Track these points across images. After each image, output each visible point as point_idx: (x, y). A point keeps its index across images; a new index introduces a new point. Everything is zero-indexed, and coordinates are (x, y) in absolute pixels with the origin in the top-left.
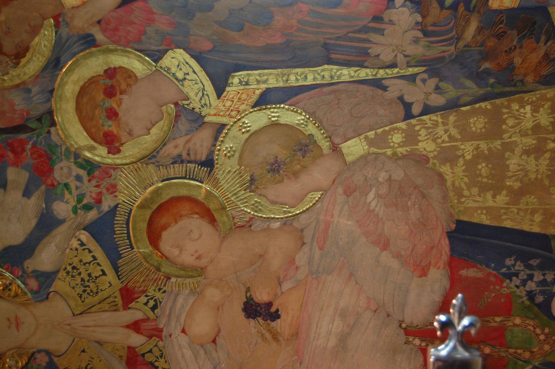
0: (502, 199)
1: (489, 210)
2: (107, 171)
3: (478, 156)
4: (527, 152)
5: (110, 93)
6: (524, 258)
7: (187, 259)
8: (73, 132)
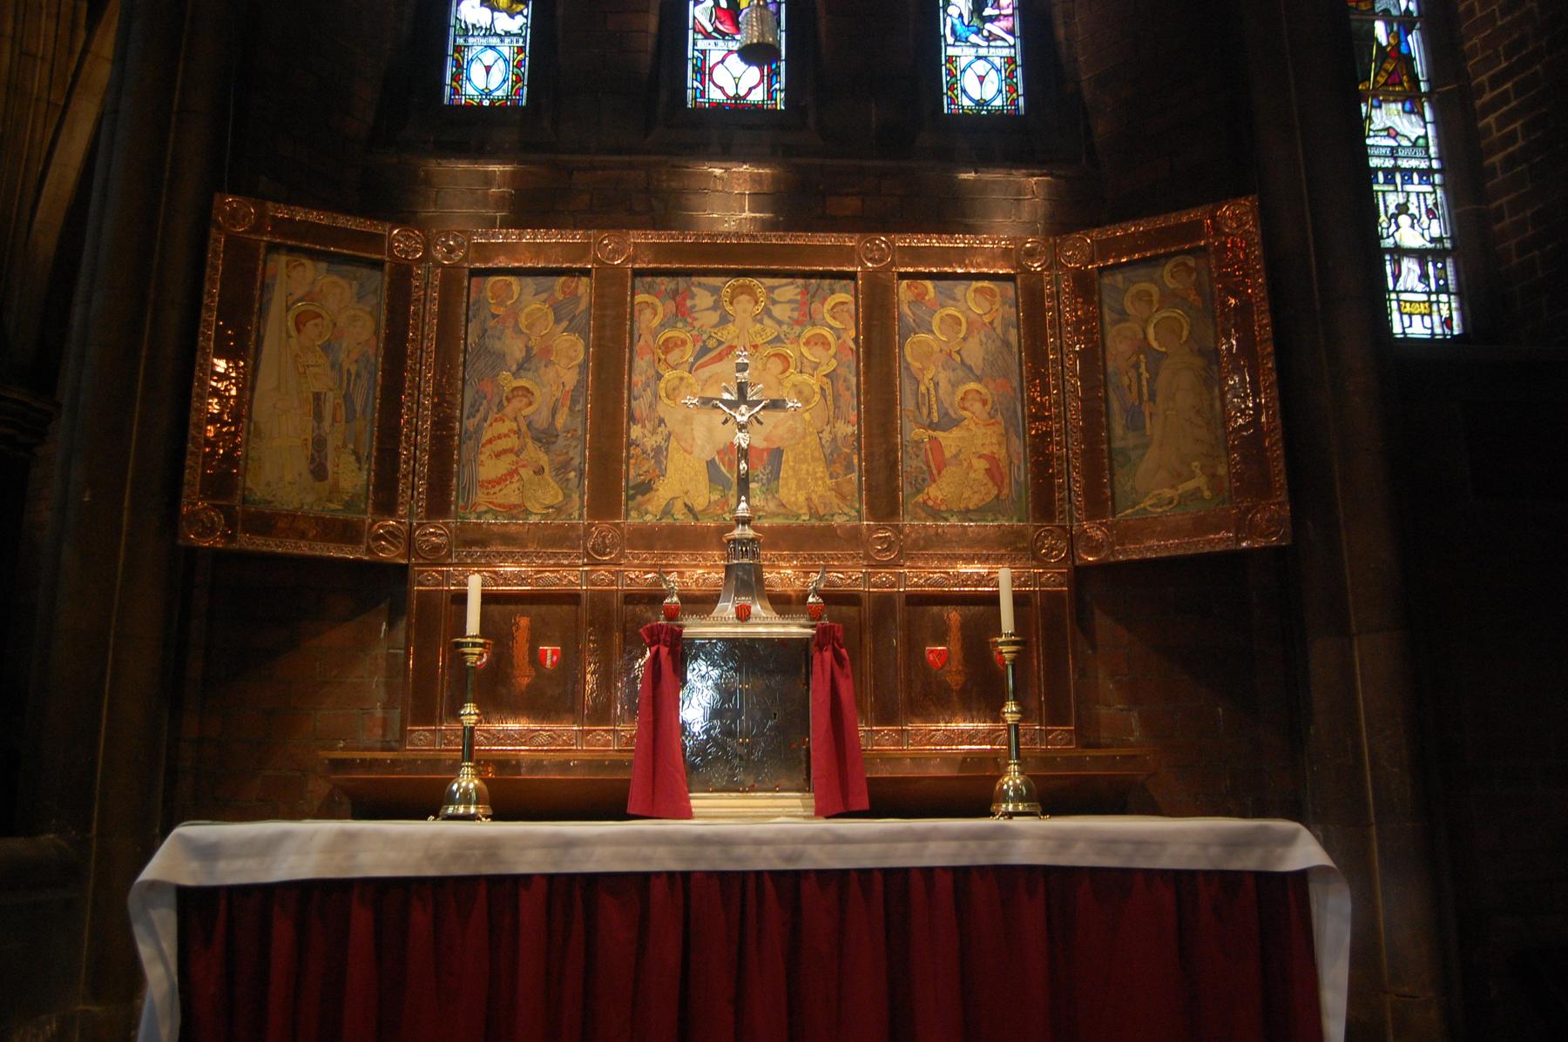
8: (809, 332)
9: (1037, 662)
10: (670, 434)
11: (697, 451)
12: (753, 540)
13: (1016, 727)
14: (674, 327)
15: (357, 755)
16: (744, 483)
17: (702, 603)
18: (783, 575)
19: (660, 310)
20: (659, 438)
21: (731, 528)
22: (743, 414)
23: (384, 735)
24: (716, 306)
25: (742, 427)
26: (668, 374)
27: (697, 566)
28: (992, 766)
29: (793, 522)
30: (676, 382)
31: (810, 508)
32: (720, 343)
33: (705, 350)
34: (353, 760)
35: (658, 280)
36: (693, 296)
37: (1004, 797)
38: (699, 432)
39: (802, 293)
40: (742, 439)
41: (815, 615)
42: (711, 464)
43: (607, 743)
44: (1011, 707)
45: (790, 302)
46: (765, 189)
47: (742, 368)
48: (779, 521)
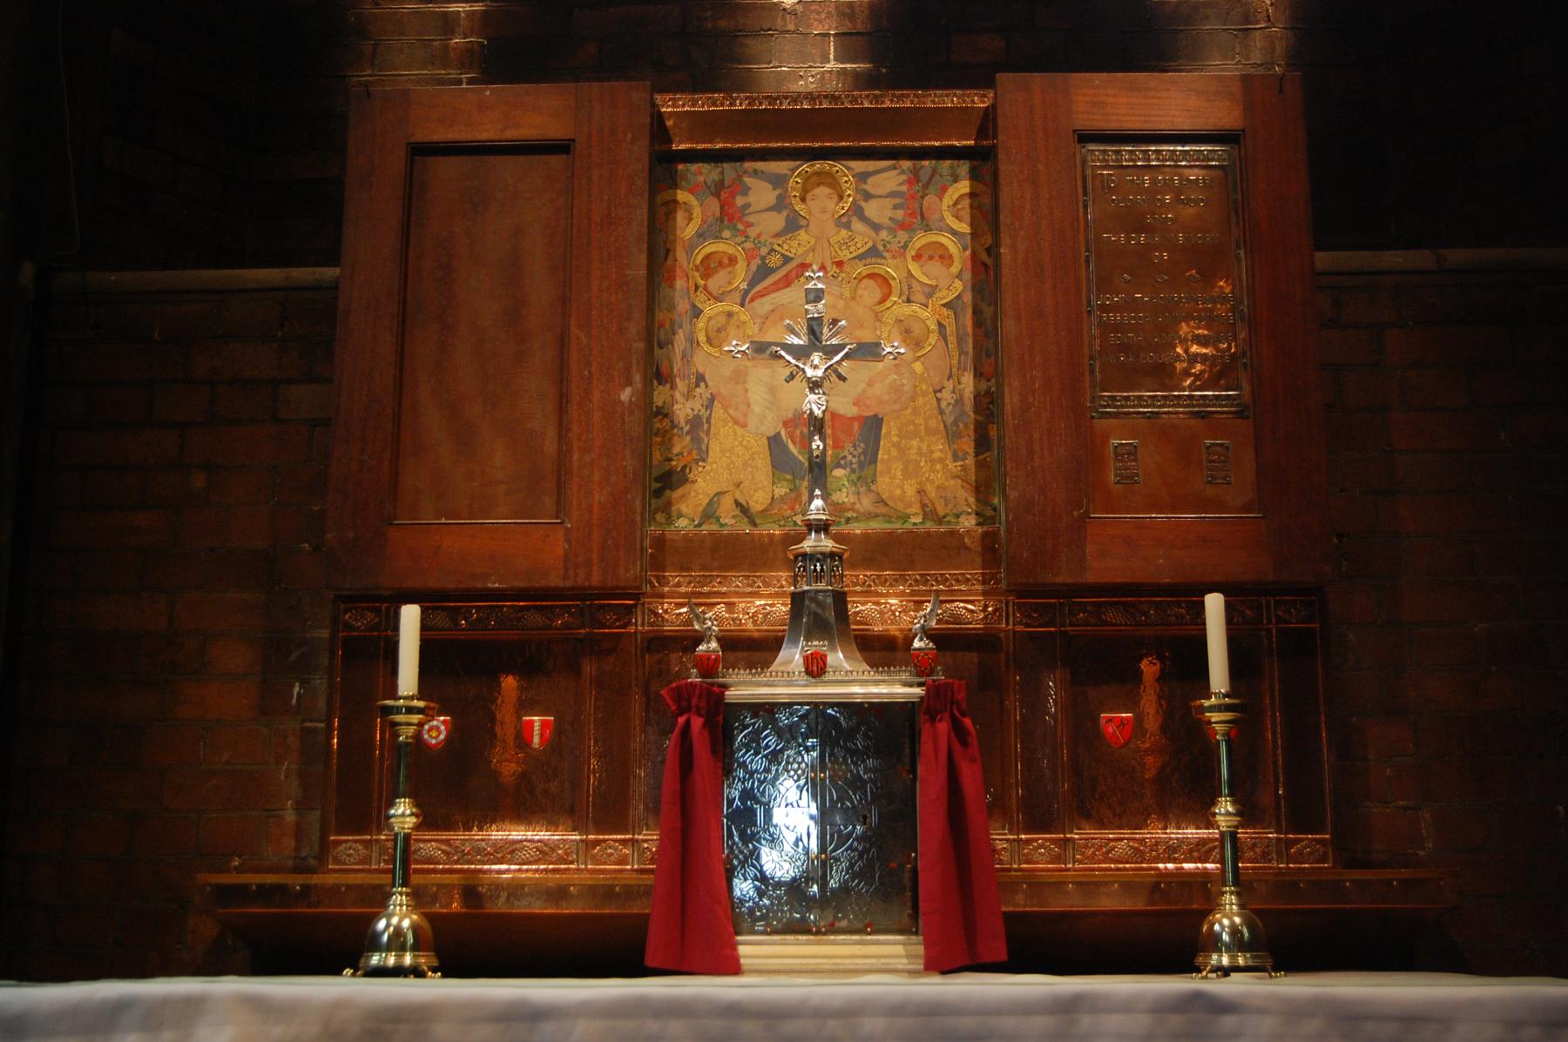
0: (895, 439)
1: (889, 433)
2: (903, 255)
3: (916, 425)
4: (919, 448)
5: (941, 257)
6: (864, 453)
7: (859, 292)
8: (921, 240)
9: (1273, 734)
10: (712, 399)
11: (752, 422)
12: (832, 555)
13: (1233, 835)
14: (718, 237)
15: (254, 879)
16: (818, 471)
17: (756, 649)
18: (886, 606)
19: (697, 212)
20: (697, 405)
21: (800, 538)
22: (815, 368)
23: (297, 849)
24: (780, 205)
25: (815, 385)
26: (710, 309)
27: (757, 595)
28: (1203, 892)
29: (897, 526)
30: (722, 319)
31: (923, 505)
32: (787, 260)
33: (764, 271)
34: (246, 887)
35: (694, 167)
36: (746, 191)
37: (1214, 943)
38: (757, 394)
39: (909, 182)
40: (814, 404)
41: (922, 668)
42: (774, 442)
43: (623, 860)
44: (1225, 808)
45: (892, 195)
46: (860, 27)
47: (817, 296)
48: (877, 526)
